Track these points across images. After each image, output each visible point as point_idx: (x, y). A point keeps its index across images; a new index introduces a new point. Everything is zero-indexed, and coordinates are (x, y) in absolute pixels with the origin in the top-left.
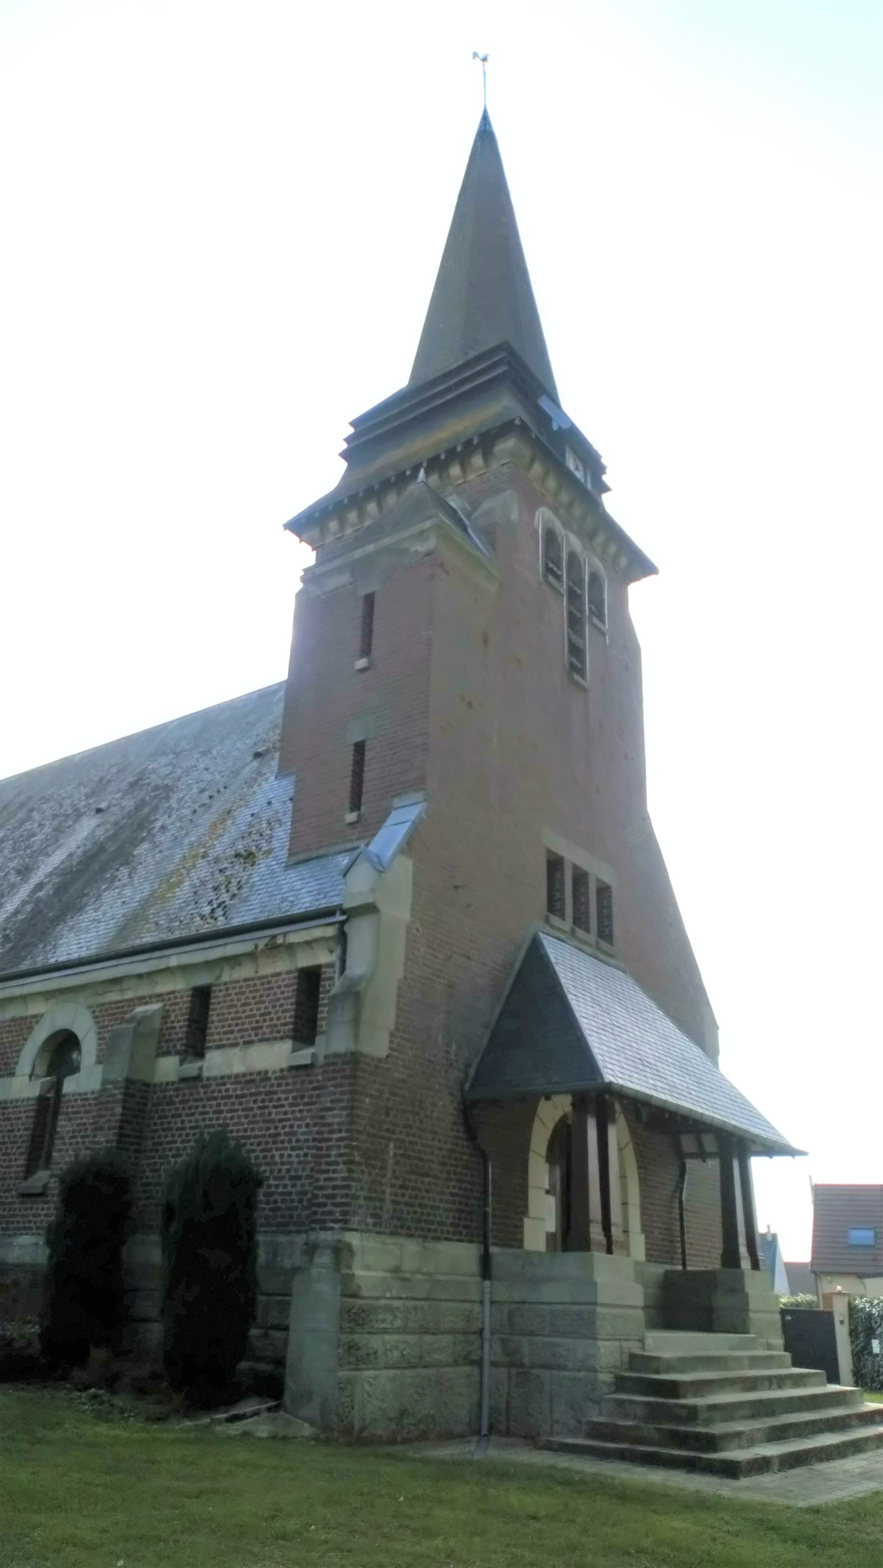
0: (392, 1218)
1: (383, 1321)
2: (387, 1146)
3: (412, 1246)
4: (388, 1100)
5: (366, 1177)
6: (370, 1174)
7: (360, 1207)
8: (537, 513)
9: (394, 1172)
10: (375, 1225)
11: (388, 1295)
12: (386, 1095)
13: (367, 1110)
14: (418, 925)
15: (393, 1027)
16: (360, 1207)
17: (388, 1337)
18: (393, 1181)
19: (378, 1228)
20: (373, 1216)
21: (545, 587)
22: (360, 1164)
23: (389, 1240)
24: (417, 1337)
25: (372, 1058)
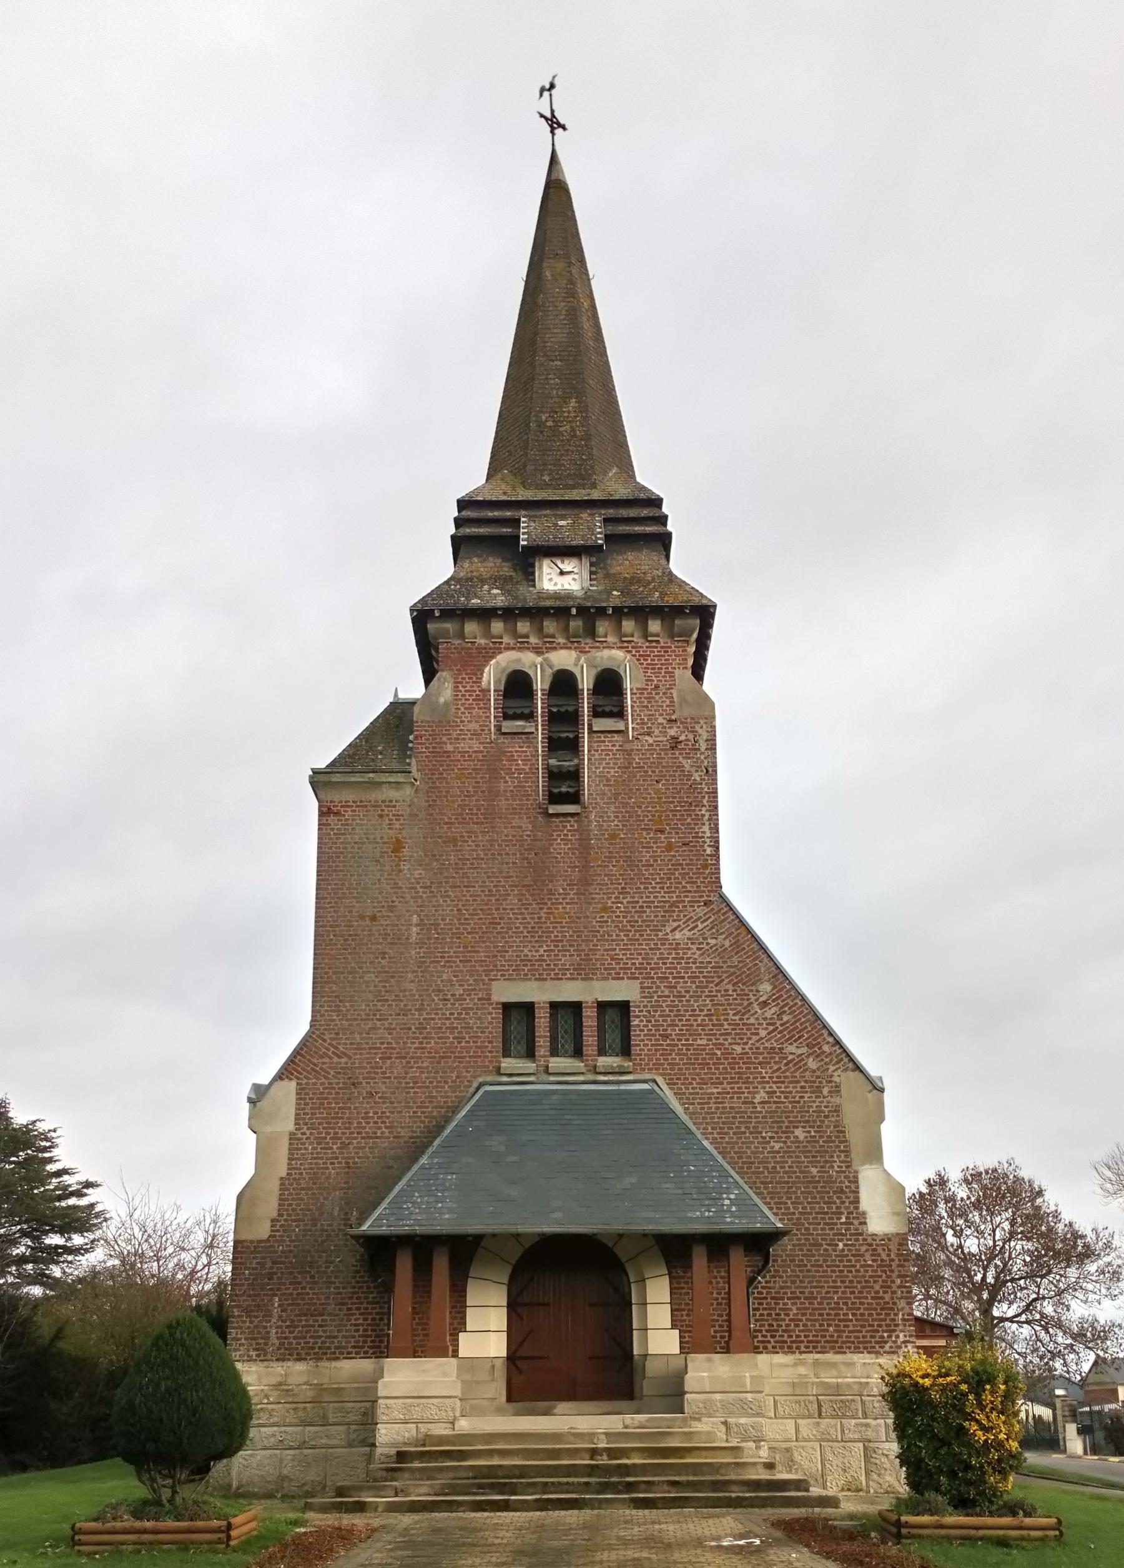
0: (278, 1349)
1: (259, 1418)
2: (271, 1300)
3: (300, 1367)
4: (272, 1268)
5: (248, 1324)
6: (251, 1322)
7: (243, 1345)
8: (487, 670)
9: (280, 1317)
10: (257, 1355)
11: (266, 1401)
12: (269, 1264)
13: (246, 1279)
14: (305, 1130)
15: (274, 1214)
16: (243, 1345)
17: (263, 1429)
18: (280, 1323)
19: (262, 1354)
20: (254, 1350)
21: (502, 739)
22: (239, 1316)
23: (275, 1364)
24: (301, 1428)
25: (252, 1242)
